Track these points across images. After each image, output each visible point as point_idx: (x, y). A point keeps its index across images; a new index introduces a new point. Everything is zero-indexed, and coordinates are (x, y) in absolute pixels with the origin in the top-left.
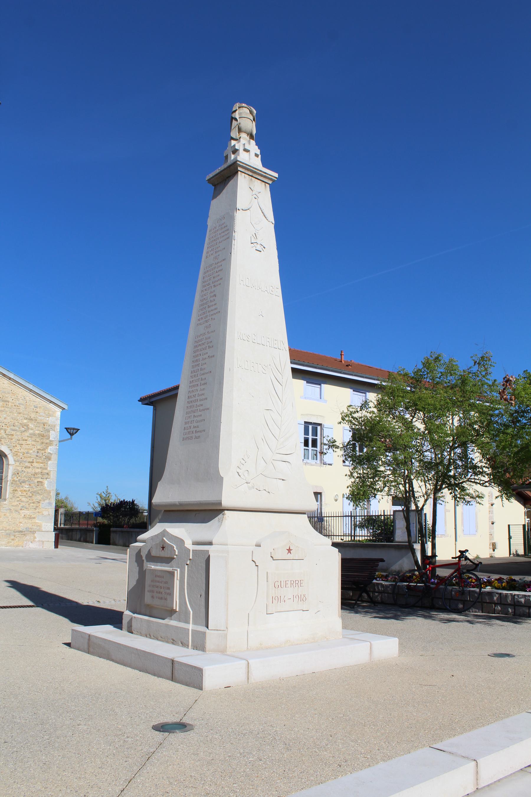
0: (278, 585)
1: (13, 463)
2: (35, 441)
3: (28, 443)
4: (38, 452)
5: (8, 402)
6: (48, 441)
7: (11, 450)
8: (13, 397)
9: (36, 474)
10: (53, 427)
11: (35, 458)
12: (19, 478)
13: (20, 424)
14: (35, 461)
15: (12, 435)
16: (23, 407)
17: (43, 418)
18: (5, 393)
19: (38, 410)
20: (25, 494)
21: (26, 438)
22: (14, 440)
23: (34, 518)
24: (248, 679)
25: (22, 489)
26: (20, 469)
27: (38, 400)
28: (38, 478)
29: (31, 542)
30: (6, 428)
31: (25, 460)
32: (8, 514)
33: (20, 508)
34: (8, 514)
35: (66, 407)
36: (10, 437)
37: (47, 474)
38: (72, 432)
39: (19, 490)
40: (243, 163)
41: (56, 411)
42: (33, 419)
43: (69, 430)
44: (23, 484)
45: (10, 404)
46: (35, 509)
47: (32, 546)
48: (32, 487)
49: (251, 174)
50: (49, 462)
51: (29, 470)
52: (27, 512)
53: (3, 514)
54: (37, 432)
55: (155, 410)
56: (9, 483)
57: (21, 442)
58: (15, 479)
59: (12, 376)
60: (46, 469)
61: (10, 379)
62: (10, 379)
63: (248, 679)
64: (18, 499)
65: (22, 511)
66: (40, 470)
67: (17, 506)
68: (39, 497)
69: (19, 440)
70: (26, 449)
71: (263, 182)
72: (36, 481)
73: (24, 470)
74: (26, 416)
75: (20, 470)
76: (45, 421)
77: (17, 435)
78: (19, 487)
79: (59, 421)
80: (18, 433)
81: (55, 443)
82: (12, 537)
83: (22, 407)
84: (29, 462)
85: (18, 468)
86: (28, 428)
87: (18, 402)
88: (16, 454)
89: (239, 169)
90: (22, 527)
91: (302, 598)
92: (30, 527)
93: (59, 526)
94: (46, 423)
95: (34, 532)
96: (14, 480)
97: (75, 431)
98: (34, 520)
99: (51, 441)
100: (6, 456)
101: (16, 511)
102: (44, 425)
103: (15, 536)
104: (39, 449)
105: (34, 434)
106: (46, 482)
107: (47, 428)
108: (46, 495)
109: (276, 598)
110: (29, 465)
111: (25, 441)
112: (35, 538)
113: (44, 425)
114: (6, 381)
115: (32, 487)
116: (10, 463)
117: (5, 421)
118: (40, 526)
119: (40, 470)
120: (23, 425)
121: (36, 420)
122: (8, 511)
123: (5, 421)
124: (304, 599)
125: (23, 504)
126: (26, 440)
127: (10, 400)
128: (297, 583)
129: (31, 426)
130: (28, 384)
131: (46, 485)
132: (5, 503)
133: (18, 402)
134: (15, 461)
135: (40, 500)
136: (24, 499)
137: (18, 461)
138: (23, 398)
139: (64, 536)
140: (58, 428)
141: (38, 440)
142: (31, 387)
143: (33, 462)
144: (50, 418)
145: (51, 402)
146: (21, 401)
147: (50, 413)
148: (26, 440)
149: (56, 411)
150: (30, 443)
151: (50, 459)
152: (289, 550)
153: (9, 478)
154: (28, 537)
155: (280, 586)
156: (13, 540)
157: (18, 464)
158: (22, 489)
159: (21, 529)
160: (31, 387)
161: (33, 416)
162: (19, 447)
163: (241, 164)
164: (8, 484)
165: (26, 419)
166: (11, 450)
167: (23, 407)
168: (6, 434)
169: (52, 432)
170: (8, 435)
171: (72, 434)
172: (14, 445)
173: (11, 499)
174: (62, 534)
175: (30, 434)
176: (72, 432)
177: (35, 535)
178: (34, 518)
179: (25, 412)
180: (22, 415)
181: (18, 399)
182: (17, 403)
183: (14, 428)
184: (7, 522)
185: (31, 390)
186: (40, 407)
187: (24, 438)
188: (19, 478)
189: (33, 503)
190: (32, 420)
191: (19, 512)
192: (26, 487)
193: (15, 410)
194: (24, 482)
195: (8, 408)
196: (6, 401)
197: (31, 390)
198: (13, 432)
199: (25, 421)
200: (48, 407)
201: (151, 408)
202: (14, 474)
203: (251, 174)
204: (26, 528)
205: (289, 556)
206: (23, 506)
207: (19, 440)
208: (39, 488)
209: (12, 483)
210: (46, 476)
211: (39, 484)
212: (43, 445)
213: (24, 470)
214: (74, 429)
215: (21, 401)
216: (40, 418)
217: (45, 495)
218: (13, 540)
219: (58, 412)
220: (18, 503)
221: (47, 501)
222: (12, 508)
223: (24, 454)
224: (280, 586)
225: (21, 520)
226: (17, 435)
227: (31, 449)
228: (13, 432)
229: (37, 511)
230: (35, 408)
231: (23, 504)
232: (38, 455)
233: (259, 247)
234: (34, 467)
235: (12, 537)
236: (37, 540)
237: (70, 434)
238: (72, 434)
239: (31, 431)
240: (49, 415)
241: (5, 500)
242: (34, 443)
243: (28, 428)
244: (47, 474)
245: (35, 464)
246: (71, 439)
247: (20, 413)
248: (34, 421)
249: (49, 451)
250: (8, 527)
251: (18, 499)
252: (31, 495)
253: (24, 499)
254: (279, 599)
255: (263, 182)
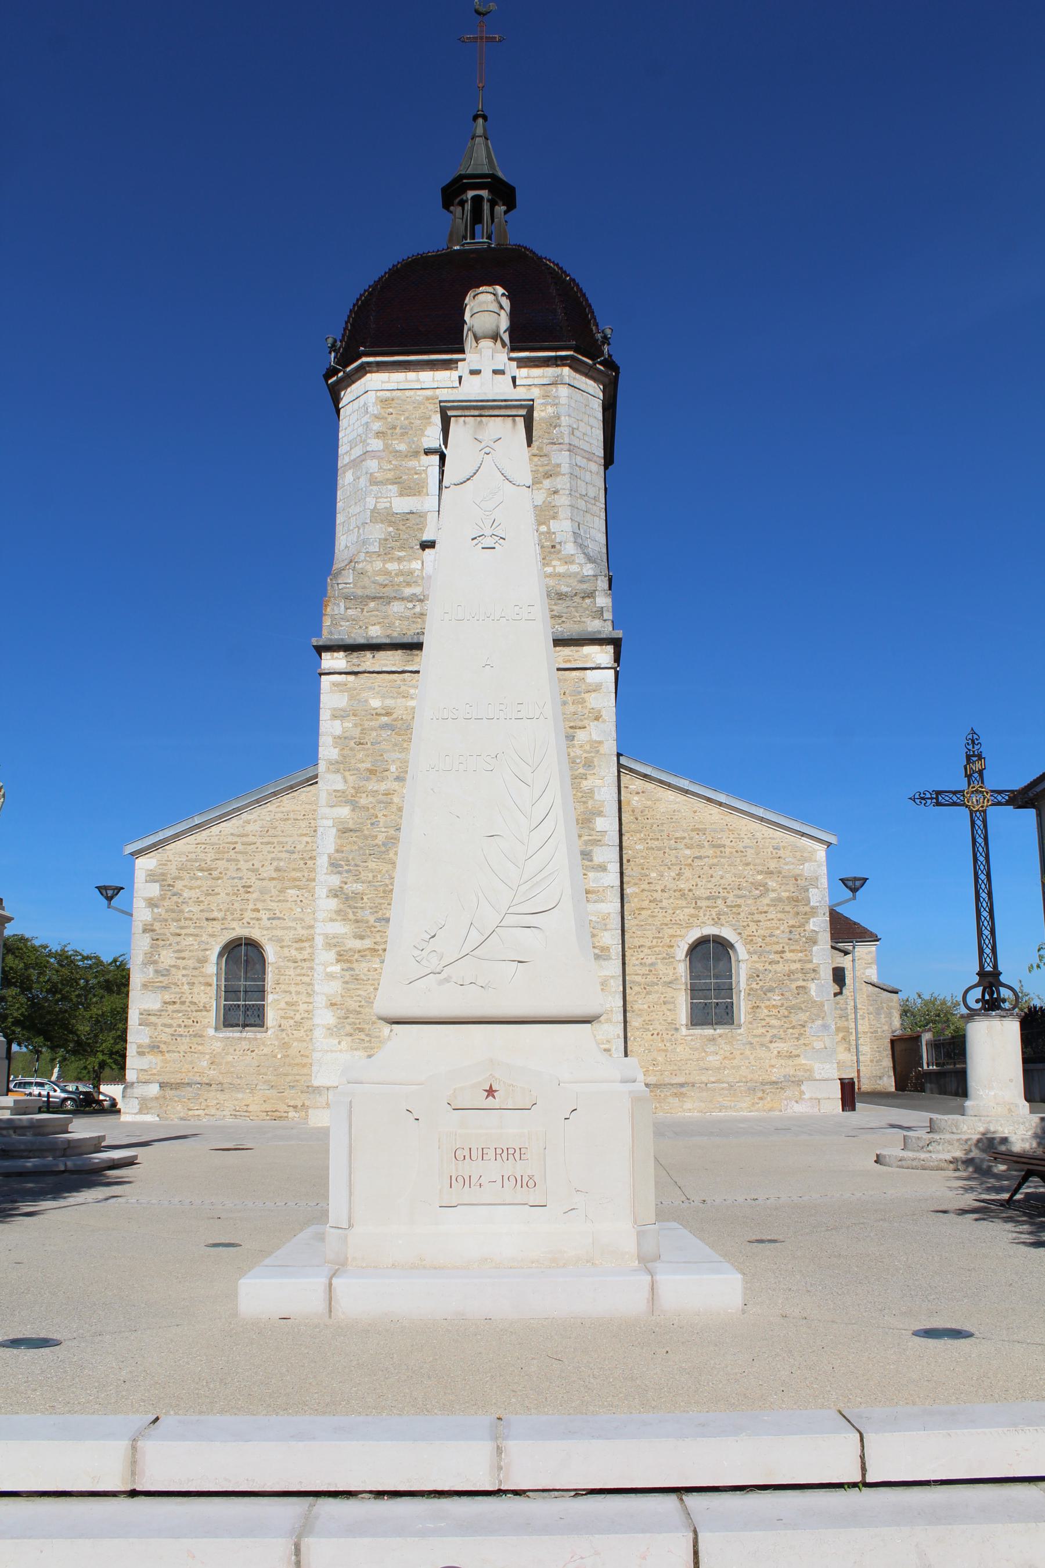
0: (462, 1154)
1: (747, 957)
2: (783, 912)
3: (770, 916)
4: (791, 932)
5: (724, 846)
6: (807, 909)
7: (740, 934)
8: (732, 836)
9: (792, 972)
10: (814, 881)
11: (788, 944)
12: (761, 983)
13: (752, 883)
14: (786, 949)
15: (739, 906)
16: (753, 851)
17: (792, 867)
18: (715, 831)
19: (781, 853)
20: (774, 1011)
21: (766, 909)
22: (742, 914)
23: (798, 1056)
24: (330, 1311)
25: (768, 1003)
26: (760, 966)
27: (779, 834)
28: (797, 980)
29: (797, 1102)
30: (726, 894)
31: (768, 948)
32: (748, 1052)
33: (768, 1038)
34: (748, 1052)
35: (833, 839)
36: (734, 910)
37: (814, 971)
38: (854, 885)
39: (763, 1005)
40: (453, 401)
41: (815, 851)
42: (775, 870)
43: (850, 883)
44: (769, 995)
45: (728, 850)
46: (798, 1039)
47: (799, 1109)
48: (787, 999)
49: (476, 413)
50: (815, 948)
51: (779, 968)
52: (782, 1045)
53: (738, 1052)
54: (785, 895)
55: (1039, 815)
56: (742, 994)
57: (757, 917)
58: (754, 986)
59: (722, 798)
60: (811, 961)
61: (721, 804)
62: (721, 804)
63: (330, 1311)
64: (763, 1023)
65: (774, 1045)
66: (798, 966)
67: (762, 1035)
68: (803, 1016)
69: (753, 914)
70: (767, 929)
71: (509, 416)
72: (793, 986)
73: (769, 967)
74: (760, 868)
75: (761, 968)
76: (798, 872)
77: (747, 905)
78: (762, 1000)
79: (824, 869)
80: (749, 902)
81: (821, 911)
82: (760, 1094)
83: (750, 851)
84: (776, 953)
85: (757, 966)
86: (767, 890)
87: (741, 844)
88: (749, 941)
89: (450, 413)
90: (776, 1074)
91: (526, 1183)
92: (791, 1073)
93: (925, 1067)
94: (799, 875)
95: (799, 1083)
96: (751, 989)
97: (858, 883)
98: (797, 1061)
99: (812, 908)
100: (732, 946)
101: (762, 1045)
102: (796, 880)
103: (763, 1091)
104: (793, 926)
105: (779, 899)
106: (813, 987)
107: (801, 886)
108: (815, 1012)
109: (460, 1179)
110: (777, 957)
111: (764, 915)
112: (802, 1093)
113: (796, 880)
114: (714, 810)
115: (787, 999)
116: (740, 958)
117: (722, 882)
118: (810, 1070)
119: (798, 966)
120: (756, 885)
121: (780, 872)
122: (748, 1047)
123: (722, 882)
124: (531, 1184)
125: (775, 1031)
126: (766, 912)
127: (727, 843)
128: (517, 1153)
129: (772, 884)
130: (754, 808)
131: (813, 993)
132: (739, 1031)
133: (741, 844)
134: (749, 952)
135: (806, 1022)
136: (774, 1022)
137: (755, 953)
138: (750, 835)
139: (933, 1086)
140: (824, 881)
141: (787, 908)
142: (760, 812)
143: (783, 952)
144: (806, 865)
145: (803, 834)
146: (746, 841)
147: (805, 855)
148: (766, 912)
149: (815, 851)
150: (773, 916)
151: (815, 943)
152: (491, 1092)
153: (743, 985)
154: (788, 1093)
155: (467, 1157)
156: (761, 1099)
157: (755, 957)
158: (768, 1003)
159: (774, 1079)
160: (760, 812)
161: (773, 865)
162: (753, 927)
163: (449, 404)
164: (742, 997)
165: (760, 872)
166: (740, 934)
167: (753, 851)
168: (728, 906)
169: (812, 891)
170: (731, 906)
171: (854, 890)
172: (745, 924)
173: (751, 1023)
174: (930, 1083)
175: (772, 900)
176: (854, 885)
177: (803, 1088)
178: (798, 1056)
179: (757, 861)
180: (752, 867)
181: (741, 839)
182: (740, 846)
183: (740, 893)
184: (747, 1067)
185: (762, 819)
186: (784, 847)
187: (761, 908)
188: (761, 983)
189: (793, 1028)
190: (772, 873)
191: (767, 1047)
192: (776, 998)
193: (738, 860)
194: (771, 990)
195: (724, 857)
196: (719, 846)
197: (762, 819)
198: (739, 901)
199: (760, 877)
200: (799, 845)
201: (1032, 813)
202: (750, 977)
203: (476, 413)
204: (785, 1076)
205: (490, 1102)
206: (774, 1036)
207: (753, 914)
208: (800, 999)
209: (749, 994)
210: (813, 975)
211: (801, 991)
212: (800, 917)
213: (769, 967)
214: (855, 879)
215: (746, 841)
216: (786, 867)
217: (814, 1011)
218: (761, 1099)
219: (820, 852)
220: (764, 1030)
221: (820, 1022)
222: (754, 1040)
223: (764, 938)
224: (467, 1157)
225: (773, 1062)
226: (747, 905)
227: (778, 928)
228: (739, 901)
229: (802, 1042)
230: (774, 852)
231: (775, 1031)
232: (792, 936)
233: (489, 542)
234: (787, 961)
235: (760, 1094)
236: (807, 1096)
237: (851, 889)
238: (854, 890)
239: (773, 895)
240: (803, 860)
241: (740, 1026)
242: (780, 915)
243: (767, 890)
244: (814, 971)
245: (788, 955)
246: (854, 898)
247: (748, 864)
248: (775, 876)
249: (812, 928)
250: (750, 1077)
251: (763, 1023)
252: (786, 1013)
253: (774, 1022)
254: (467, 1182)
255: (509, 416)
